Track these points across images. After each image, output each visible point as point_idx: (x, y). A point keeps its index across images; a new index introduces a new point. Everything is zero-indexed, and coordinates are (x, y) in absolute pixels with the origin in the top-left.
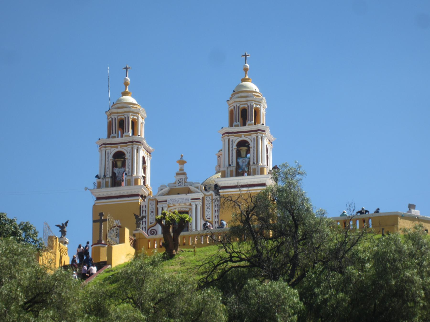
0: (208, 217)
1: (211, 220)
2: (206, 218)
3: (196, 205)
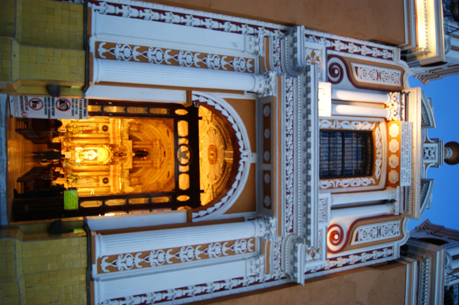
0: (360, 236)
1: (353, 243)
2: (361, 228)
3: (393, 201)
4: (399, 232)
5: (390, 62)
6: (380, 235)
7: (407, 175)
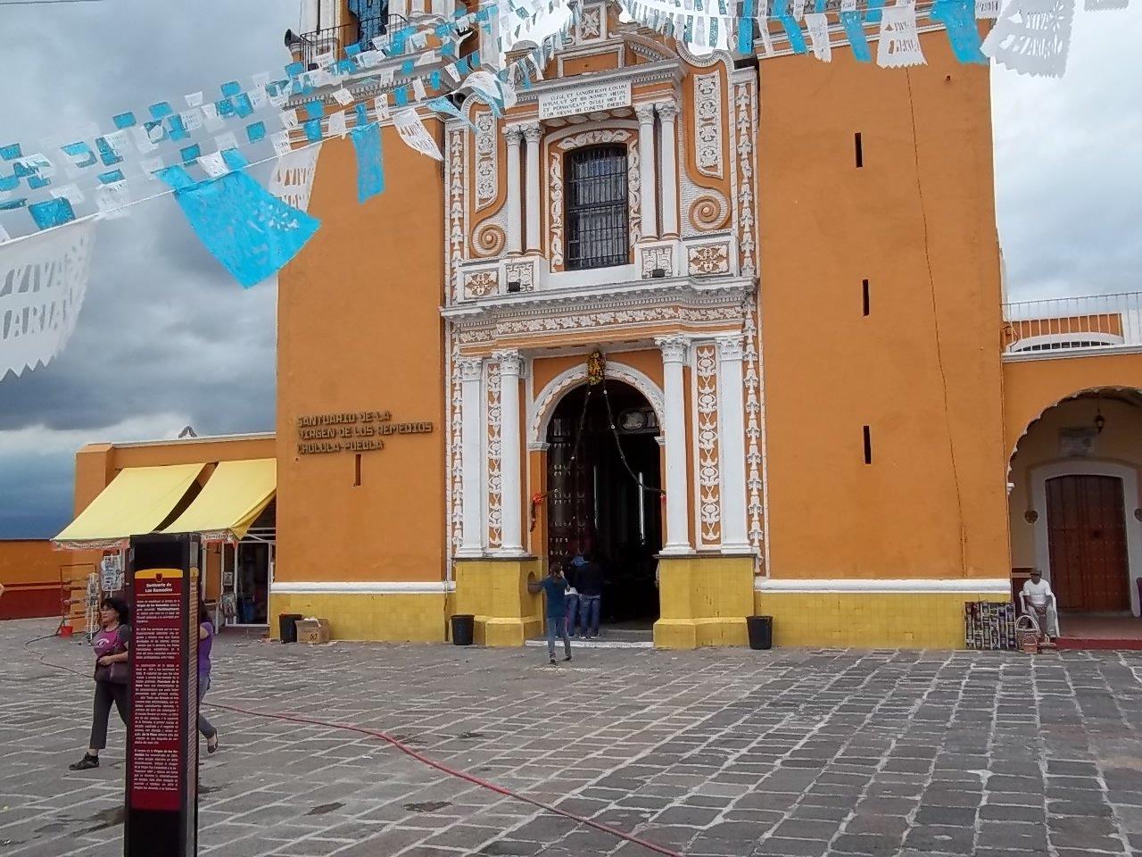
1: (720, 173)
2: (699, 164)
3: (656, 114)
4: (712, 74)
5: (466, 136)
6: (713, 118)
7: (614, 94)
